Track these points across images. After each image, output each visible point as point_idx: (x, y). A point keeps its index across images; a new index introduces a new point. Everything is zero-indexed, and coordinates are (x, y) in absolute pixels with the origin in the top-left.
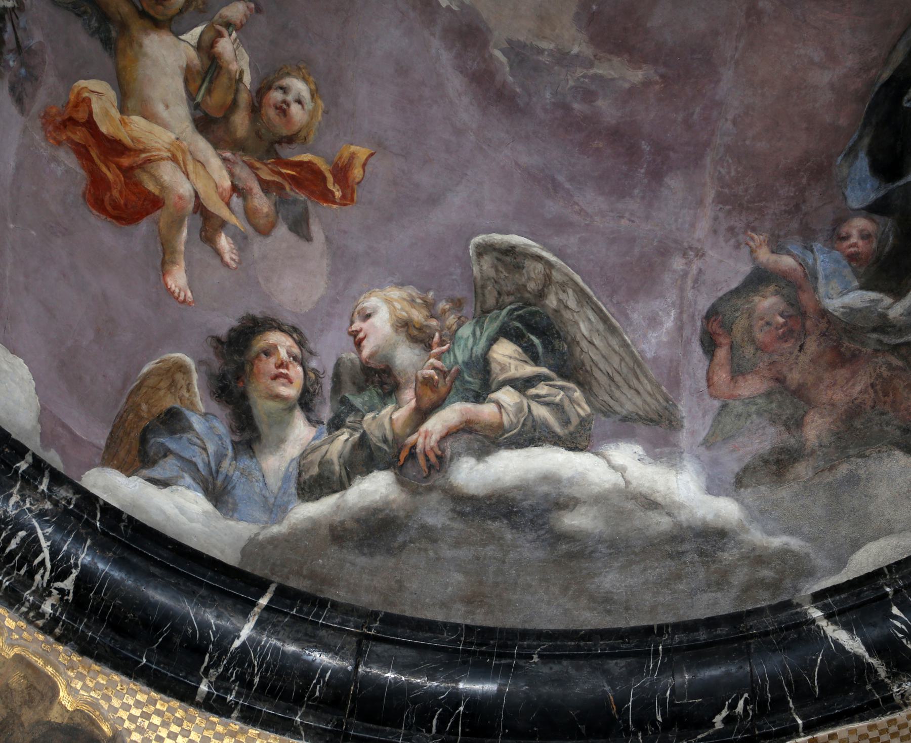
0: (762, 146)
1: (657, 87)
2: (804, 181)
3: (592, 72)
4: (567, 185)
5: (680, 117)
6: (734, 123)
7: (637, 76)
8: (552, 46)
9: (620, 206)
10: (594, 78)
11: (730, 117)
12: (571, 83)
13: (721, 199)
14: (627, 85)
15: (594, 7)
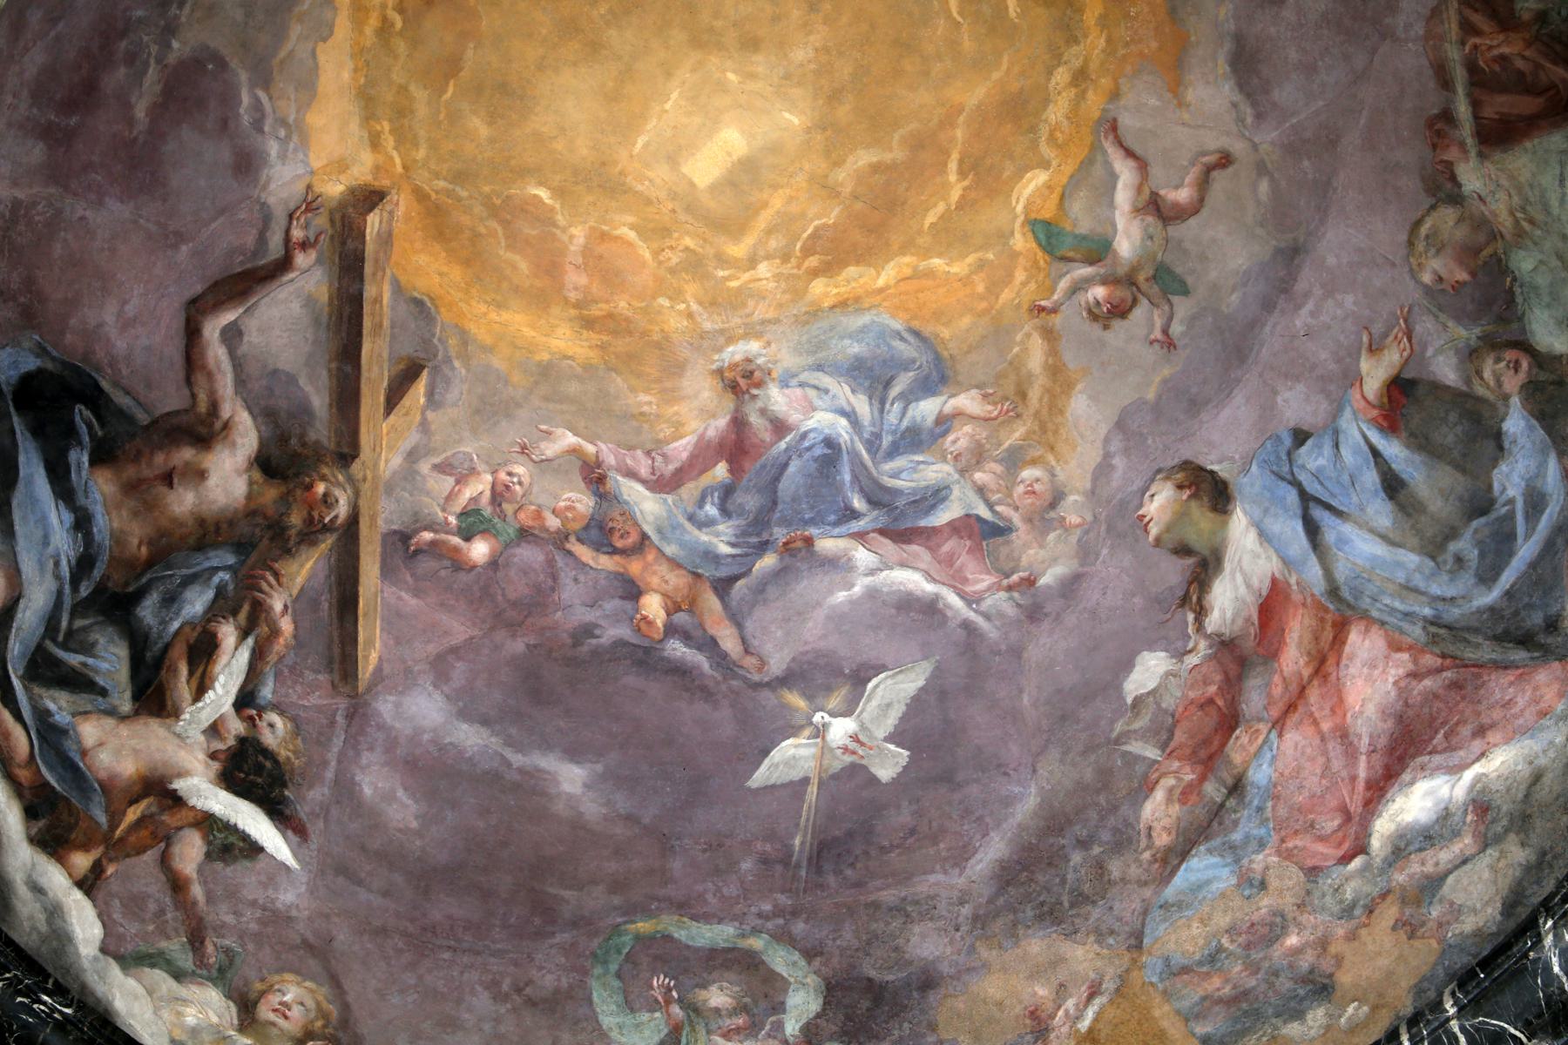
0: (58, 249)
1: (127, 133)
2: (22, 299)
3: (152, 61)
4: (52, 34)
5: (95, 158)
6: (82, 218)
7: (140, 112)
8: (183, 19)
9: (25, 93)
10: (146, 64)
11: (88, 213)
12: (146, 39)
13: (16, 204)
14: (133, 100)
15: (210, 67)
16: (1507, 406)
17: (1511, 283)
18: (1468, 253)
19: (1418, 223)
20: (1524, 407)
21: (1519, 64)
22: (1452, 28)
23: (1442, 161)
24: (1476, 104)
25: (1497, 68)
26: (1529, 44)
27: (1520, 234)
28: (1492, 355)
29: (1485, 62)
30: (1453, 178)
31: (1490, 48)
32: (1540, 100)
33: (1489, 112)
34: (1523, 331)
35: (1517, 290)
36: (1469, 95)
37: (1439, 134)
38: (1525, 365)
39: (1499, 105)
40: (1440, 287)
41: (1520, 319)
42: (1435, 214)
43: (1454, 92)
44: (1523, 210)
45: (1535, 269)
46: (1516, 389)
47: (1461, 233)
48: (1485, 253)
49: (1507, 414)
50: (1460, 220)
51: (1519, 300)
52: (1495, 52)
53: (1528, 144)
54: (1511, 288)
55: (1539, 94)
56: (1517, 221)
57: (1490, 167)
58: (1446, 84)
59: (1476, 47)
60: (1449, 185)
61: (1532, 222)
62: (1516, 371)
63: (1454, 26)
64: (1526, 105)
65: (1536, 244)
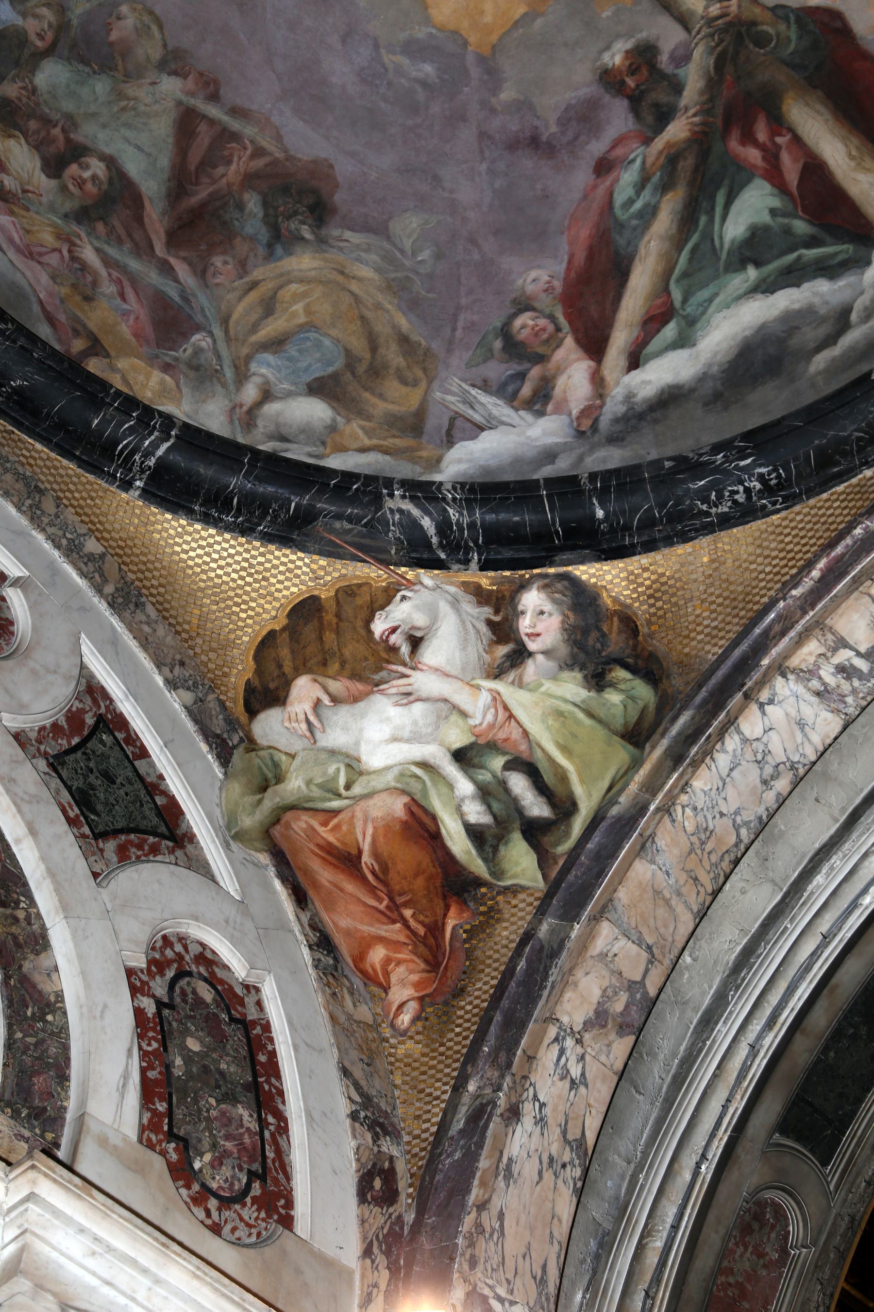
16: (18, 13)
17: (92, 68)
18: (125, 50)
19: (161, 27)
20: (13, 25)
21: (221, 170)
22: (265, 142)
23: (190, 73)
24: (212, 122)
25: (226, 153)
26: (229, 185)
27: (121, 95)
28: (55, 23)
29: (233, 148)
30: (175, 73)
31: (240, 158)
32: (192, 167)
33: (203, 128)
34: (60, 57)
35: (87, 70)
36: (219, 122)
37: (207, 84)
38: (39, 43)
39: (204, 136)
40: (114, 14)
41: (68, 60)
42: (160, 43)
43: (226, 113)
44: (134, 109)
45: (94, 92)
46: (26, 27)
47: (140, 53)
48: (120, 62)
49: (14, 8)
50: (148, 58)
51: (81, 67)
52: (235, 159)
53: (171, 140)
54: (90, 66)
55: (197, 169)
56: (128, 99)
57: (171, 104)
58: (236, 112)
59: (245, 149)
60: (173, 67)
61: (123, 109)
62: (38, 34)
63: (264, 144)
64: (195, 157)
65: (109, 103)
